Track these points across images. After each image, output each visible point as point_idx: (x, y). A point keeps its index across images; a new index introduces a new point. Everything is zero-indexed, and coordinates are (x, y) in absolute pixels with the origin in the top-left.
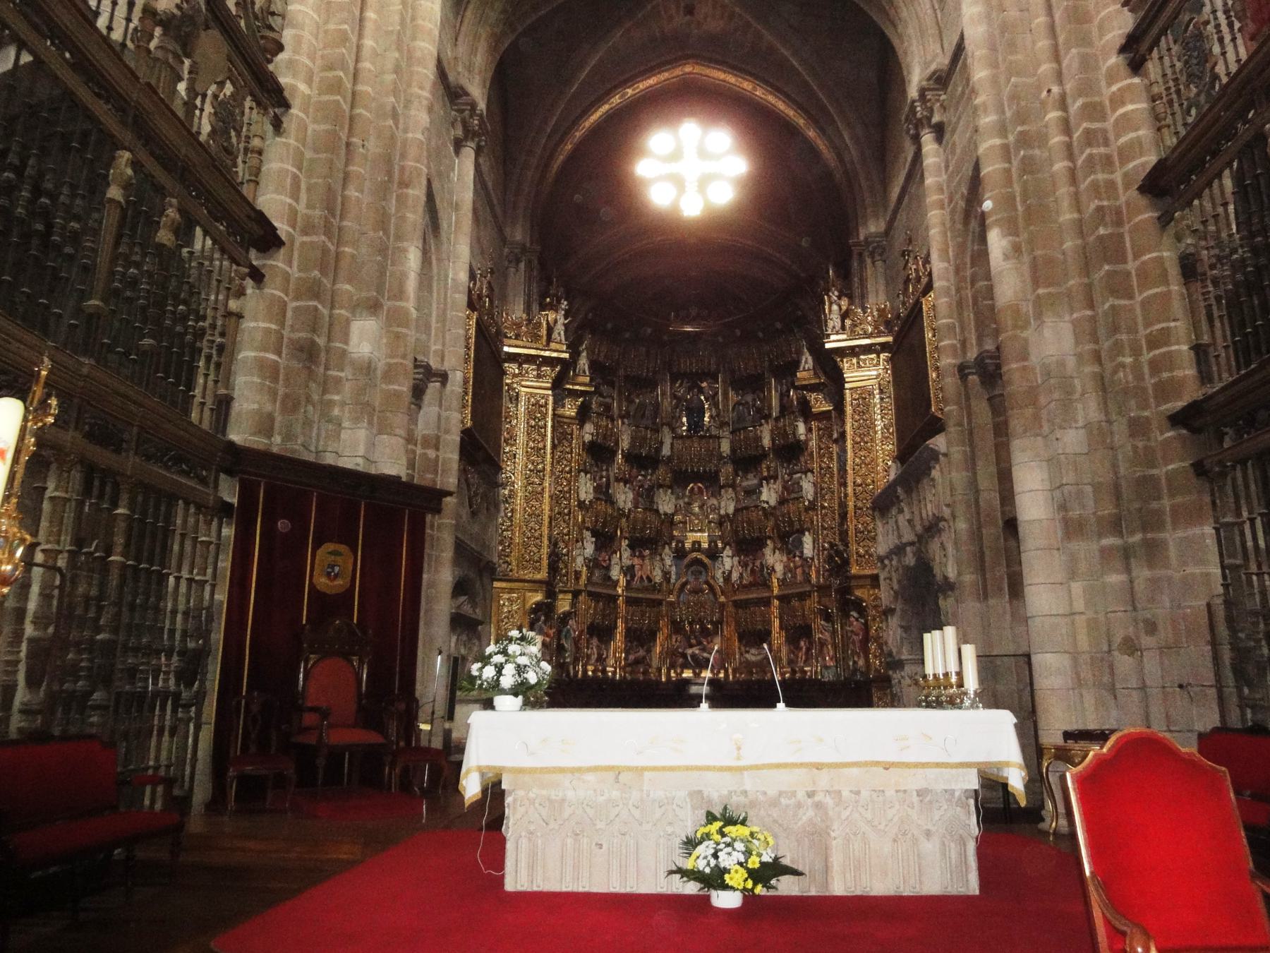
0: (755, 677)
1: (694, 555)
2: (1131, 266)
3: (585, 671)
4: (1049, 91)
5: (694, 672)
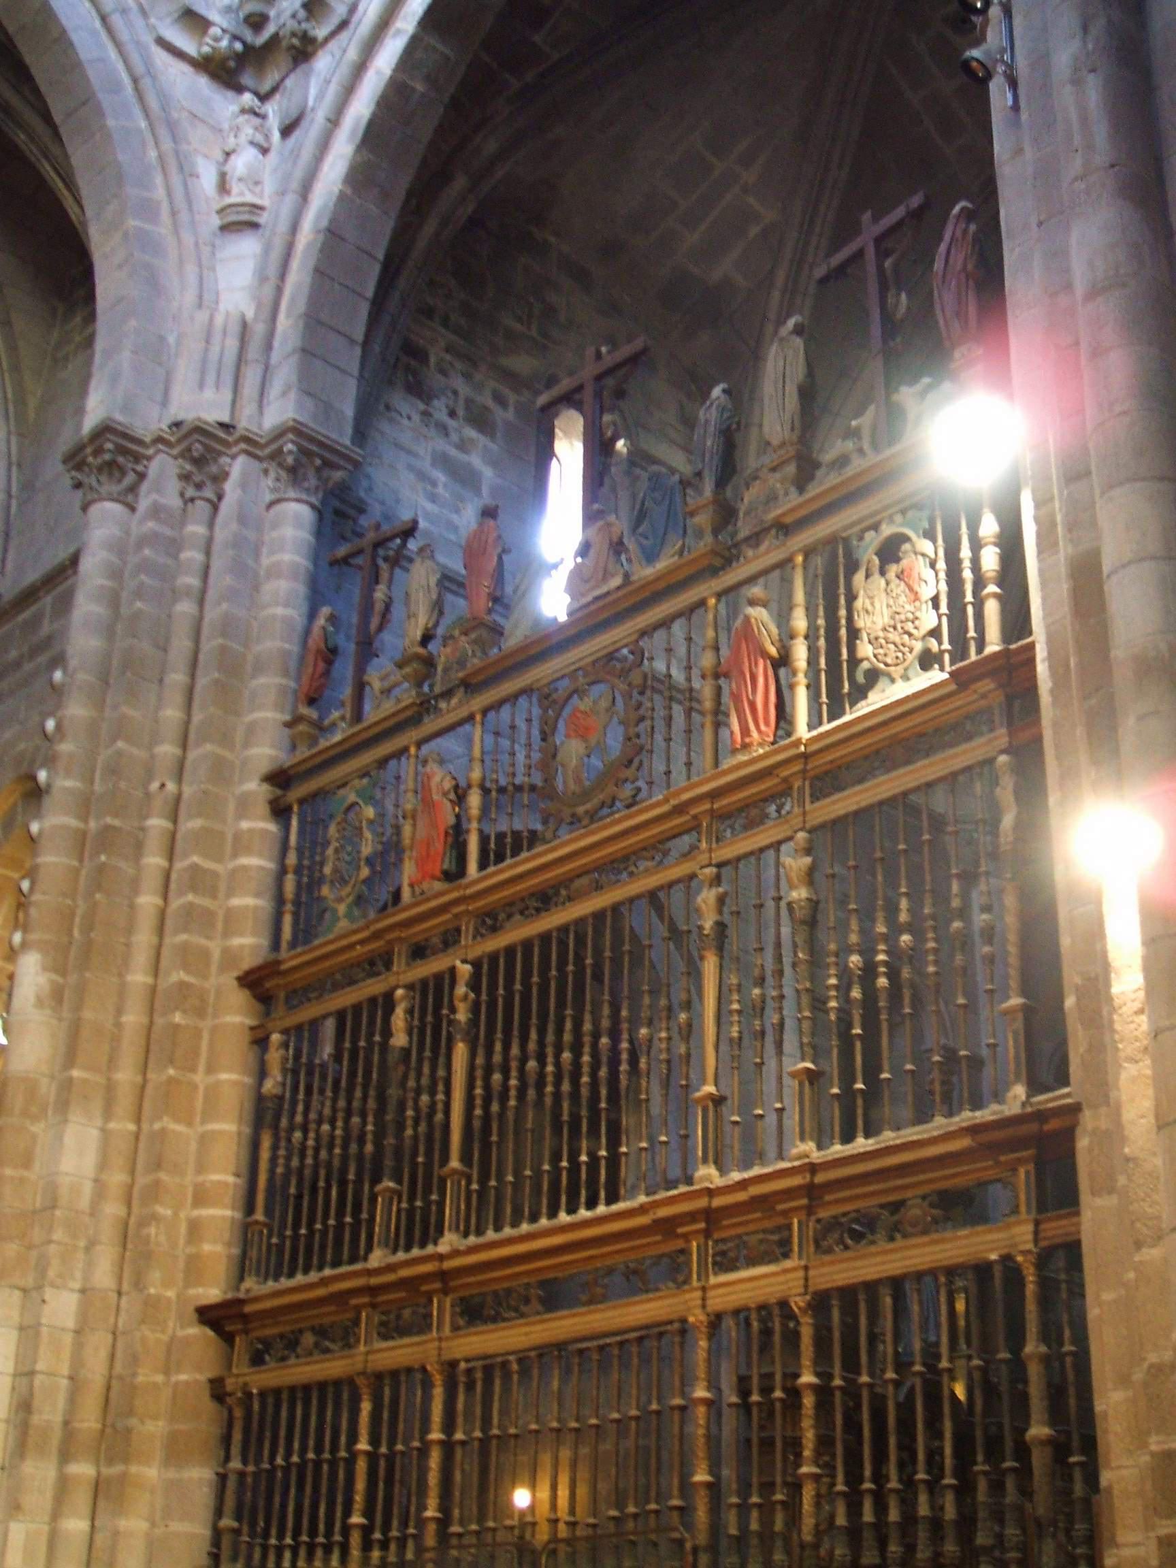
2: (199, 1078)
4: (163, 785)
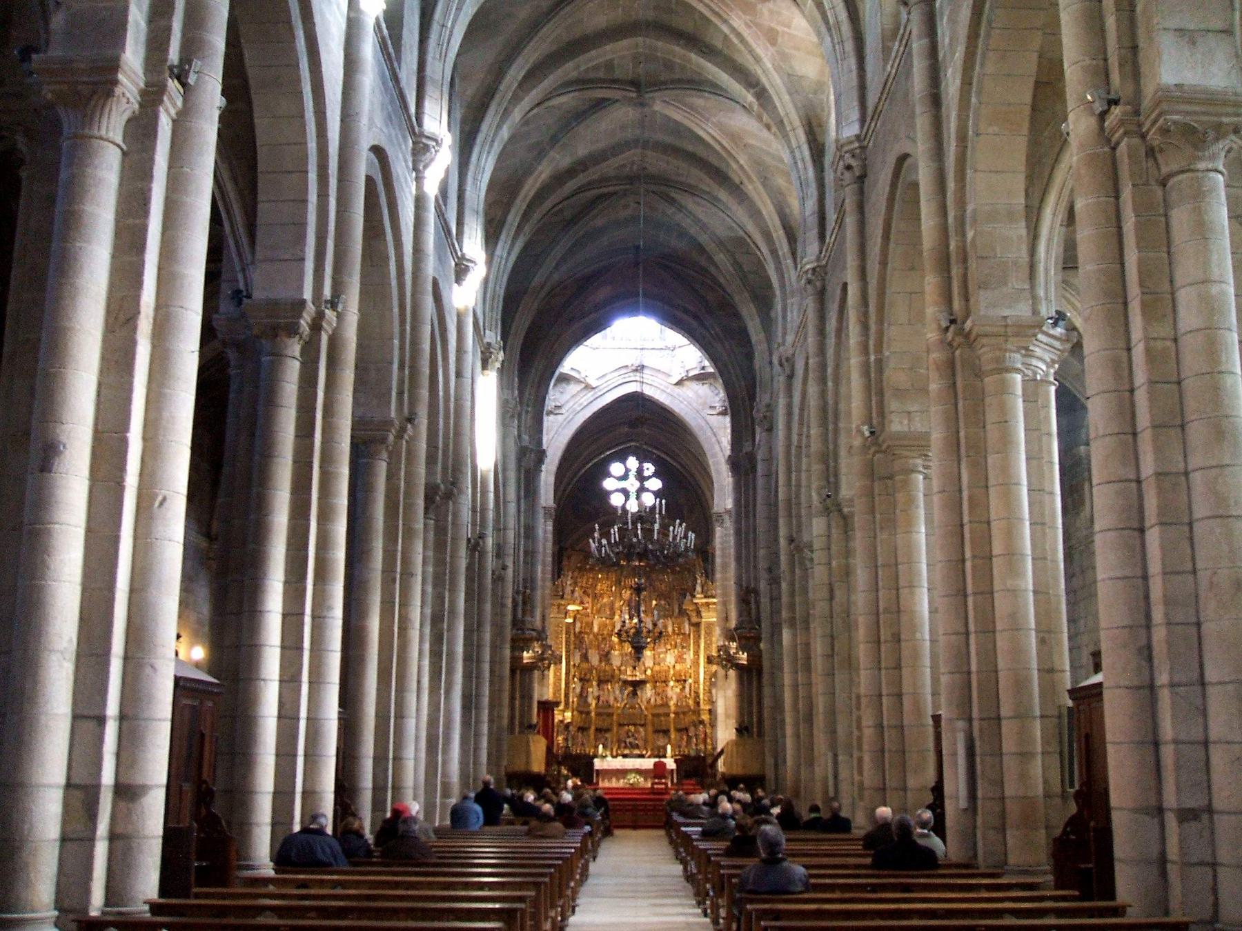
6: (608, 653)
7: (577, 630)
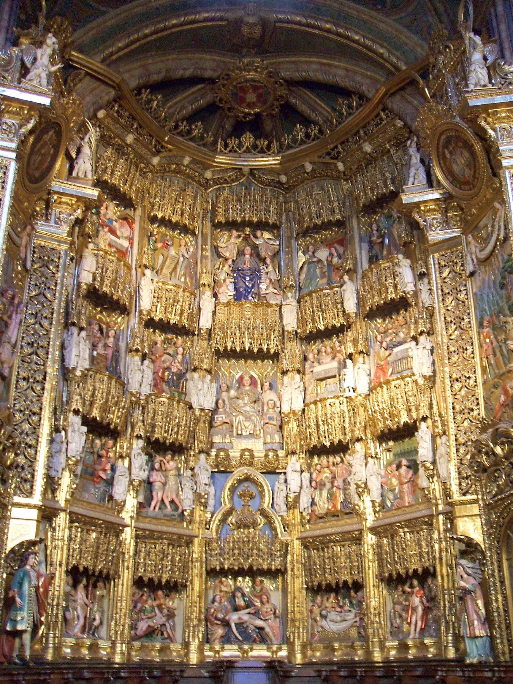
0: (338, 656)
1: (245, 470)
3: (57, 649)
5: (241, 649)
6: (181, 376)
7: (86, 278)
